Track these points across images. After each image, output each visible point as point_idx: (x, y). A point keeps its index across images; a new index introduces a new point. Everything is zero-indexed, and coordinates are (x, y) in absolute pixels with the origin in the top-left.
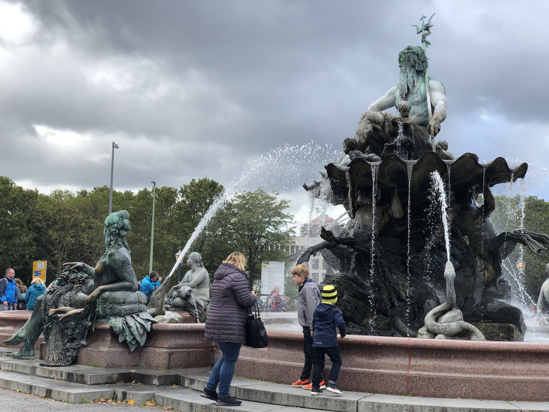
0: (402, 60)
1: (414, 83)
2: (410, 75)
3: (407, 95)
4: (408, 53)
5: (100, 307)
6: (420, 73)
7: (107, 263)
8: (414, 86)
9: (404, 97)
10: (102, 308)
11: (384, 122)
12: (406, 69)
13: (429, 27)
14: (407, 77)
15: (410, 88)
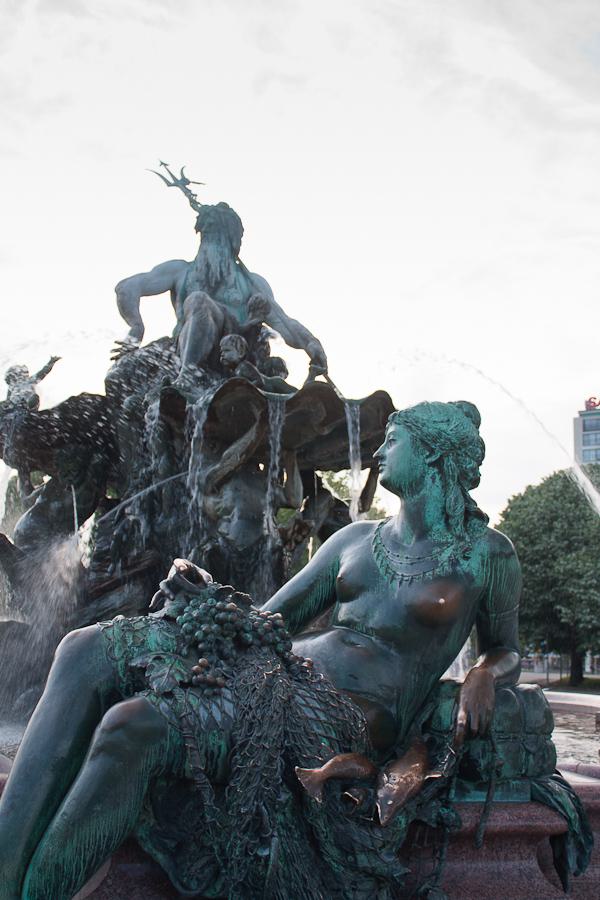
0: (212, 221)
1: (229, 268)
2: (227, 251)
3: (218, 284)
4: (224, 213)
5: (499, 747)
6: (235, 252)
7: (479, 583)
8: (229, 274)
9: (213, 285)
10: (507, 752)
11: (225, 322)
12: (220, 240)
13: (188, 182)
14: (222, 254)
15: (225, 274)
